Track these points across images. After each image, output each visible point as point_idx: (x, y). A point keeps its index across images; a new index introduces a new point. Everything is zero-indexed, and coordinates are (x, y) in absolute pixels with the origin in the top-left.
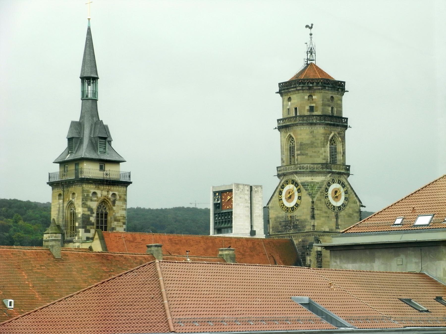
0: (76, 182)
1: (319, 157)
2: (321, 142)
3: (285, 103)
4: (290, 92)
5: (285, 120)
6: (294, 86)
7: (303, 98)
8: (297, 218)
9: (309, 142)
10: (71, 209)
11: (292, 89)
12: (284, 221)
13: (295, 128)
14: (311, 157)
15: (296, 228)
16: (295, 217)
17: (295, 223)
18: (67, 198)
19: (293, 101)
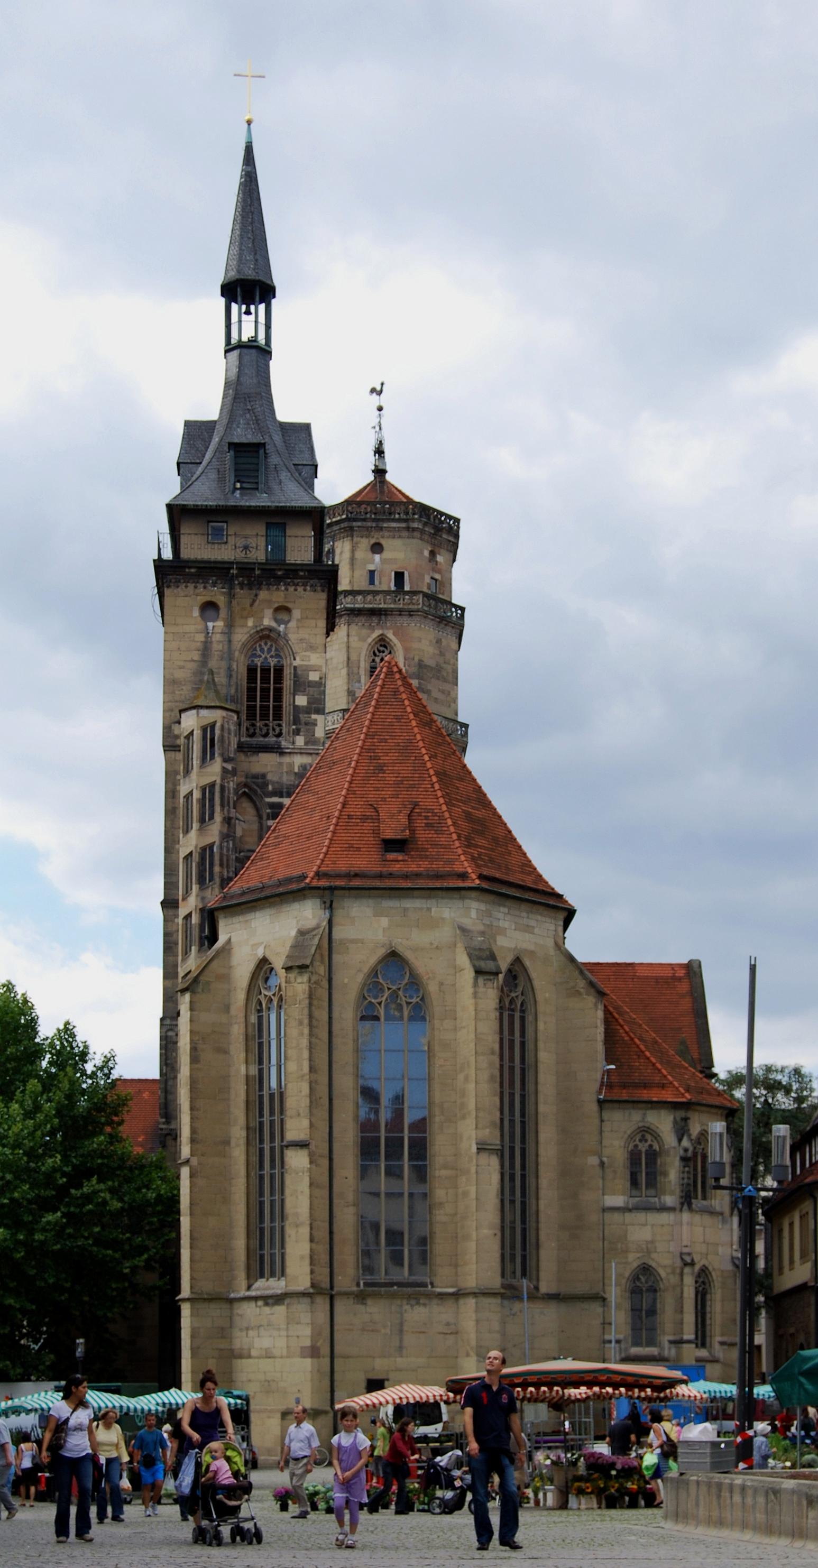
0: (302, 573)
3: (359, 555)
4: (381, 529)
5: (345, 597)
6: (403, 516)
7: (422, 553)
9: (432, 663)
10: (254, 655)
11: (394, 525)
13: (404, 621)
18: (246, 618)
19: (387, 554)
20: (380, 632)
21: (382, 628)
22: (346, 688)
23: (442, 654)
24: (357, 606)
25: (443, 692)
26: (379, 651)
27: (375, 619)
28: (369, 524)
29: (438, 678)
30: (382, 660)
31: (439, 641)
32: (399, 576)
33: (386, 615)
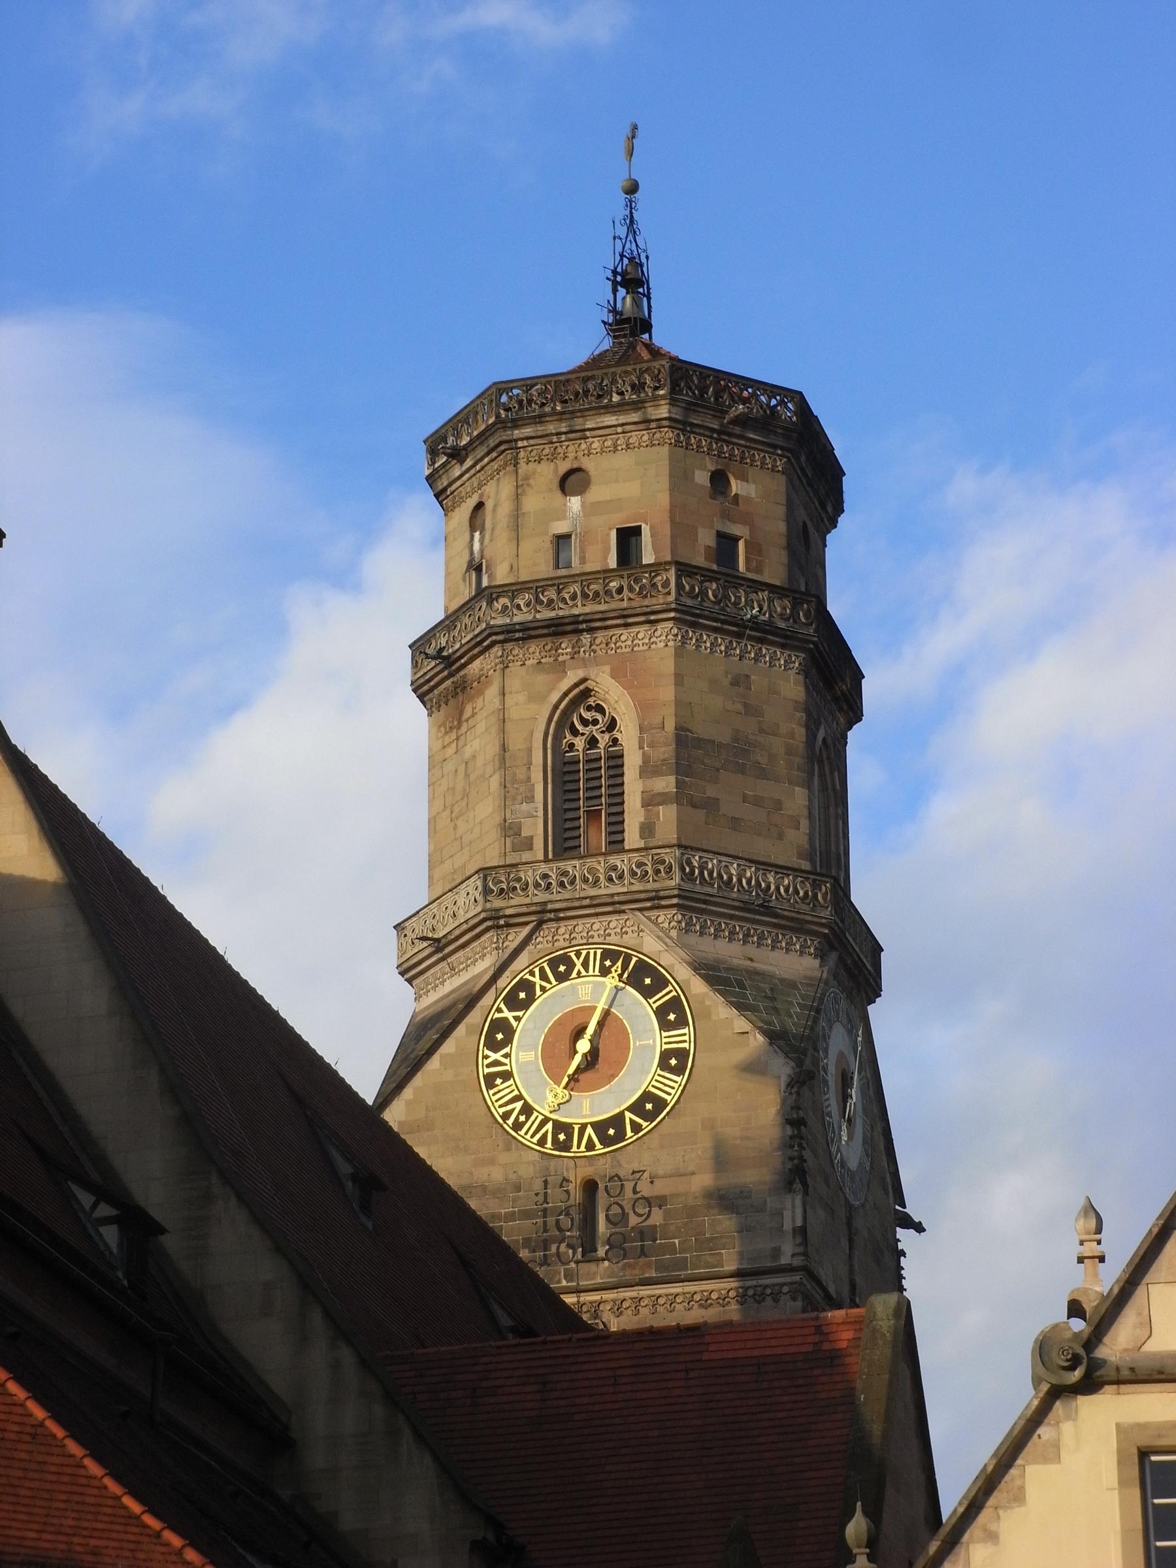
1: (781, 836)
2: (790, 752)
3: (532, 503)
4: (581, 434)
6: (630, 396)
8: (645, 1189)
9: (723, 735)
11: (610, 420)
12: (526, 1215)
14: (735, 823)
15: (643, 1253)
16: (629, 1186)
17: (633, 1220)
19: (598, 492)
20: (580, 674)
21: (584, 663)
22: (498, 819)
23: (750, 710)
24: (516, 619)
25: (758, 802)
26: (585, 722)
27: (566, 646)
28: (551, 428)
29: (741, 770)
30: (592, 742)
31: (740, 681)
32: (628, 537)
33: (591, 630)
